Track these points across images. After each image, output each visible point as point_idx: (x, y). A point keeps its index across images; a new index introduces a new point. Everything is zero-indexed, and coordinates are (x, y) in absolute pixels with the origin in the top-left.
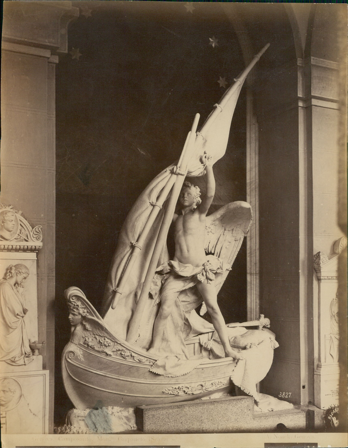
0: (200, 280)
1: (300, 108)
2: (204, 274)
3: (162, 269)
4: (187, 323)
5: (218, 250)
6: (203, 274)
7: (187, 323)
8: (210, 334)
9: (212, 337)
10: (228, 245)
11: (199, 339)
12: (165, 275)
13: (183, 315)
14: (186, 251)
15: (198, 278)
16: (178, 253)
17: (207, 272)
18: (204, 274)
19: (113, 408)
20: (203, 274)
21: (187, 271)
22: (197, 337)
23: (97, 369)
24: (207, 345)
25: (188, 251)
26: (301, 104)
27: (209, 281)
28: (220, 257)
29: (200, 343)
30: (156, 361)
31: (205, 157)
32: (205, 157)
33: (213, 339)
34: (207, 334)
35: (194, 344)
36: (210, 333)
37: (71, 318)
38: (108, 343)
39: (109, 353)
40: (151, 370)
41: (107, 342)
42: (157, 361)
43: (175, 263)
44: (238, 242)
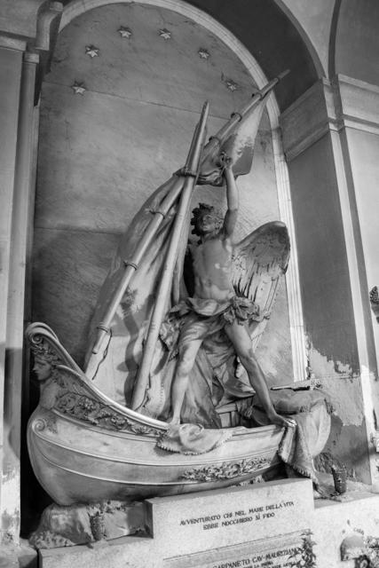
1: (331, 132)
2: (233, 311)
4: (216, 383)
5: (252, 292)
6: (231, 313)
7: (216, 383)
8: (250, 399)
18: (233, 311)
19: (109, 503)
20: (231, 312)
21: (209, 309)
26: (332, 126)
27: (240, 322)
30: (166, 431)
39: (92, 420)
43: (193, 300)
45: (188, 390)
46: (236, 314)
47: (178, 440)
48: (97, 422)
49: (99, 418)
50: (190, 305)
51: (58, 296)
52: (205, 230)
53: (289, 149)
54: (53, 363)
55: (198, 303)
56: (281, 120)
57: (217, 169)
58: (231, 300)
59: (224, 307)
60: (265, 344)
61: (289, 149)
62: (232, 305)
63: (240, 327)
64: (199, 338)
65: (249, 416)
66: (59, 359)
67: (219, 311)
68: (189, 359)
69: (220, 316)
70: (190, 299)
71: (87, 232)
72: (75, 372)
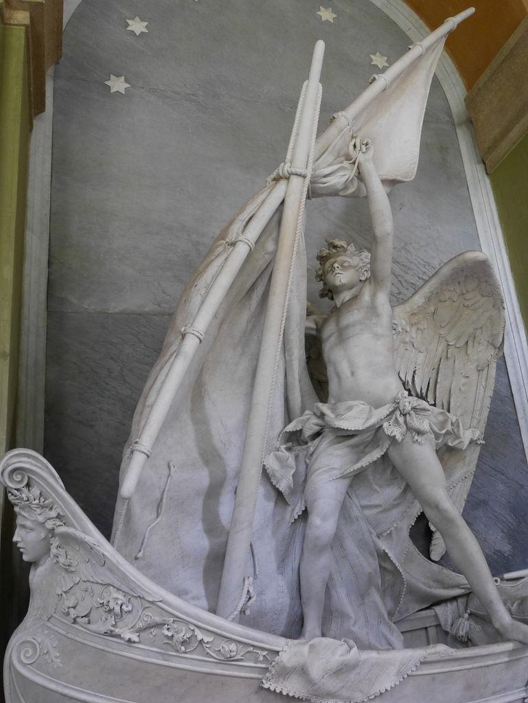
0: (392, 435)
2: (401, 419)
3: (300, 427)
9: (466, 609)
10: (463, 385)
11: (436, 616)
12: (309, 444)
13: (372, 544)
14: (348, 374)
15: (386, 430)
16: (333, 387)
17: (408, 416)
20: (397, 421)
21: (354, 418)
22: (429, 612)
23: (99, 692)
24: (458, 629)
25: (353, 373)
28: (451, 411)
29: (439, 626)
30: (278, 653)
31: (355, 146)
32: (355, 146)
33: (469, 611)
34: (455, 603)
35: (426, 628)
36: (460, 600)
37: (19, 540)
38: (120, 602)
39: (127, 635)
40: (266, 686)
41: (117, 599)
42: (280, 654)
44: (485, 371)
45: (331, 578)
46: (405, 422)
47: (302, 671)
48: (135, 638)
49: (140, 631)
50: (322, 416)
51: (91, 426)
52: (338, 283)
53: (491, 149)
54: (49, 525)
55: (333, 410)
56: (470, 102)
57: (346, 164)
58: (396, 402)
59: (385, 411)
60: (481, 497)
61: (491, 149)
62: (397, 408)
63: (416, 447)
64: (343, 477)
65: (461, 633)
66: (59, 517)
67: (373, 421)
68: (324, 519)
69: (377, 431)
70: (320, 405)
71: (140, 314)
72: (88, 539)
